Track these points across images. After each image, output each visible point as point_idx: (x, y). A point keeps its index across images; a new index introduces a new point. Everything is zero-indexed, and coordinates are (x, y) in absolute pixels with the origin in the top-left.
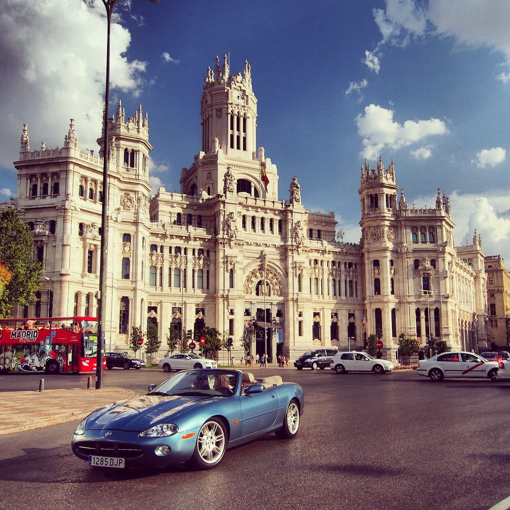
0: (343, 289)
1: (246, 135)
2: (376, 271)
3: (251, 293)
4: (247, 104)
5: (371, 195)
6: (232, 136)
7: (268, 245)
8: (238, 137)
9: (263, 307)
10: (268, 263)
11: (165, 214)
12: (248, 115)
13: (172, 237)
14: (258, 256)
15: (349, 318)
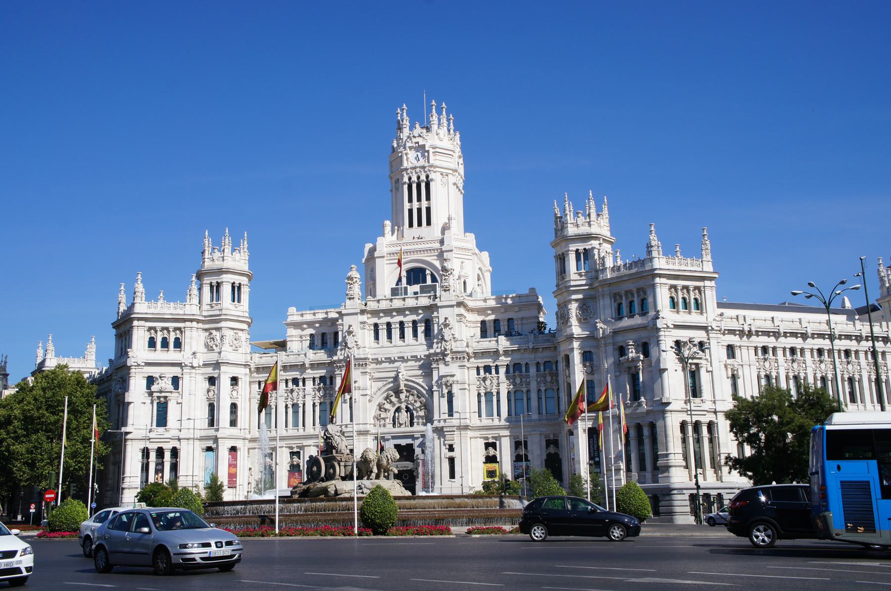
0: (534, 403)
1: (429, 204)
2: (567, 371)
3: (384, 426)
4: (428, 162)
5: (559, 255)
6: (411, 211)
7: (406, 358)
8: (419, 210)
9: (403, 442)
10: (406, 382)
11: (294, 339)
12: (430, 177)
13: (285, 368)
14: (393, 374)
15: (547, 448)
